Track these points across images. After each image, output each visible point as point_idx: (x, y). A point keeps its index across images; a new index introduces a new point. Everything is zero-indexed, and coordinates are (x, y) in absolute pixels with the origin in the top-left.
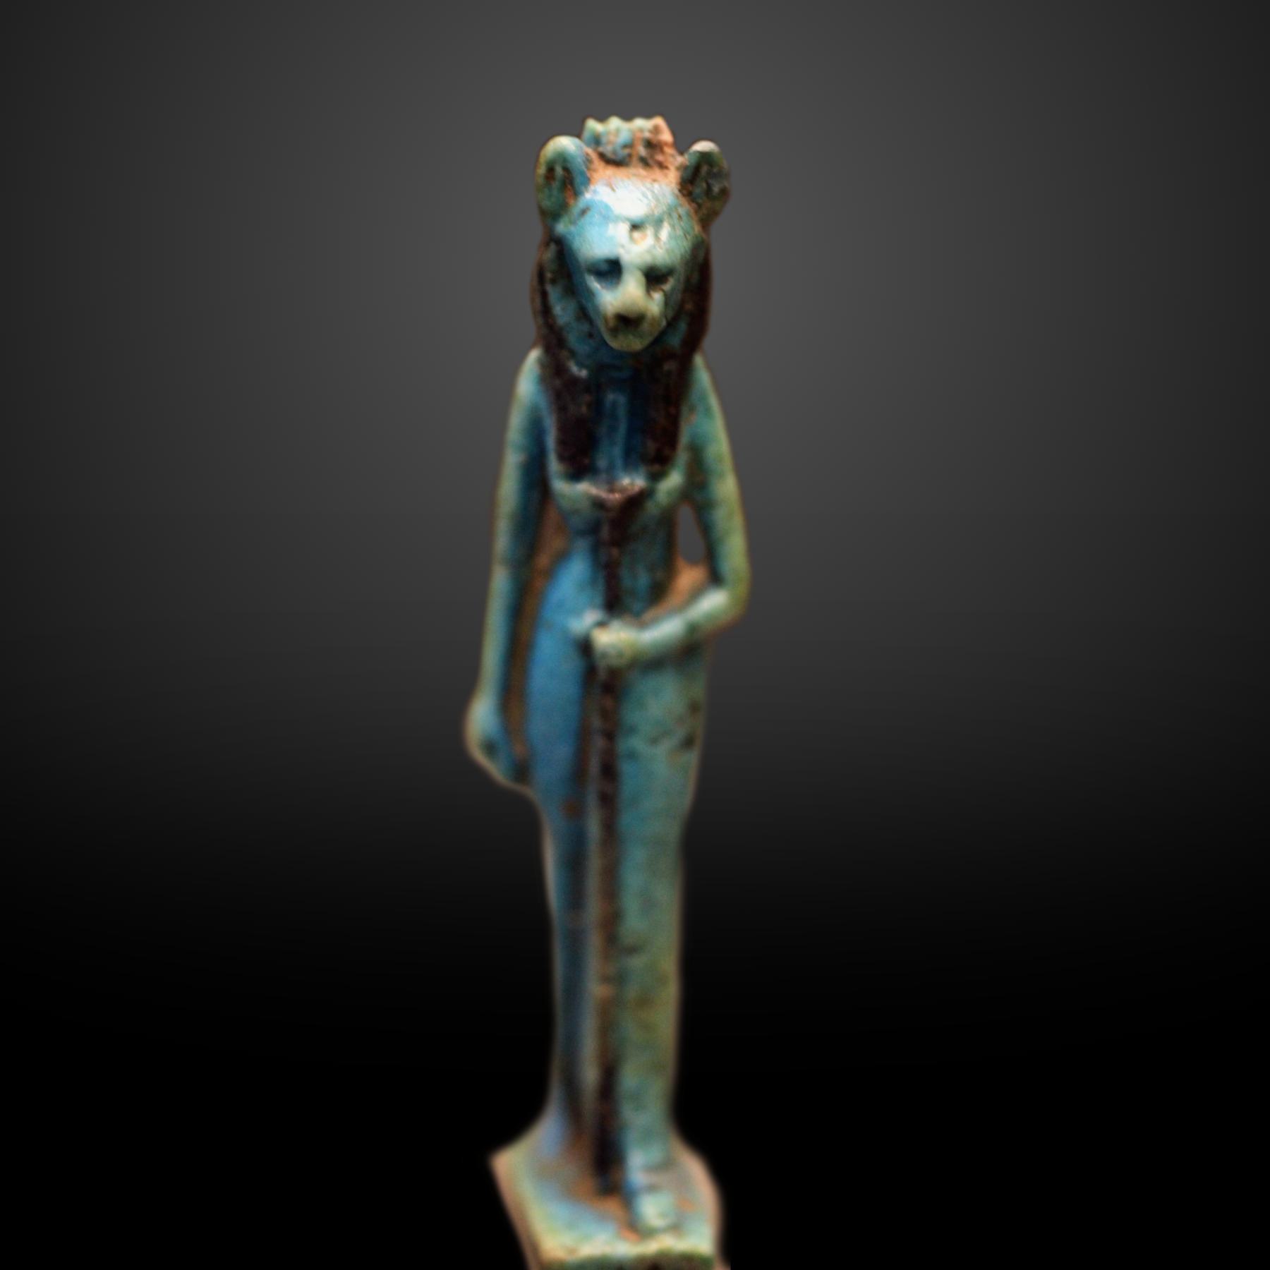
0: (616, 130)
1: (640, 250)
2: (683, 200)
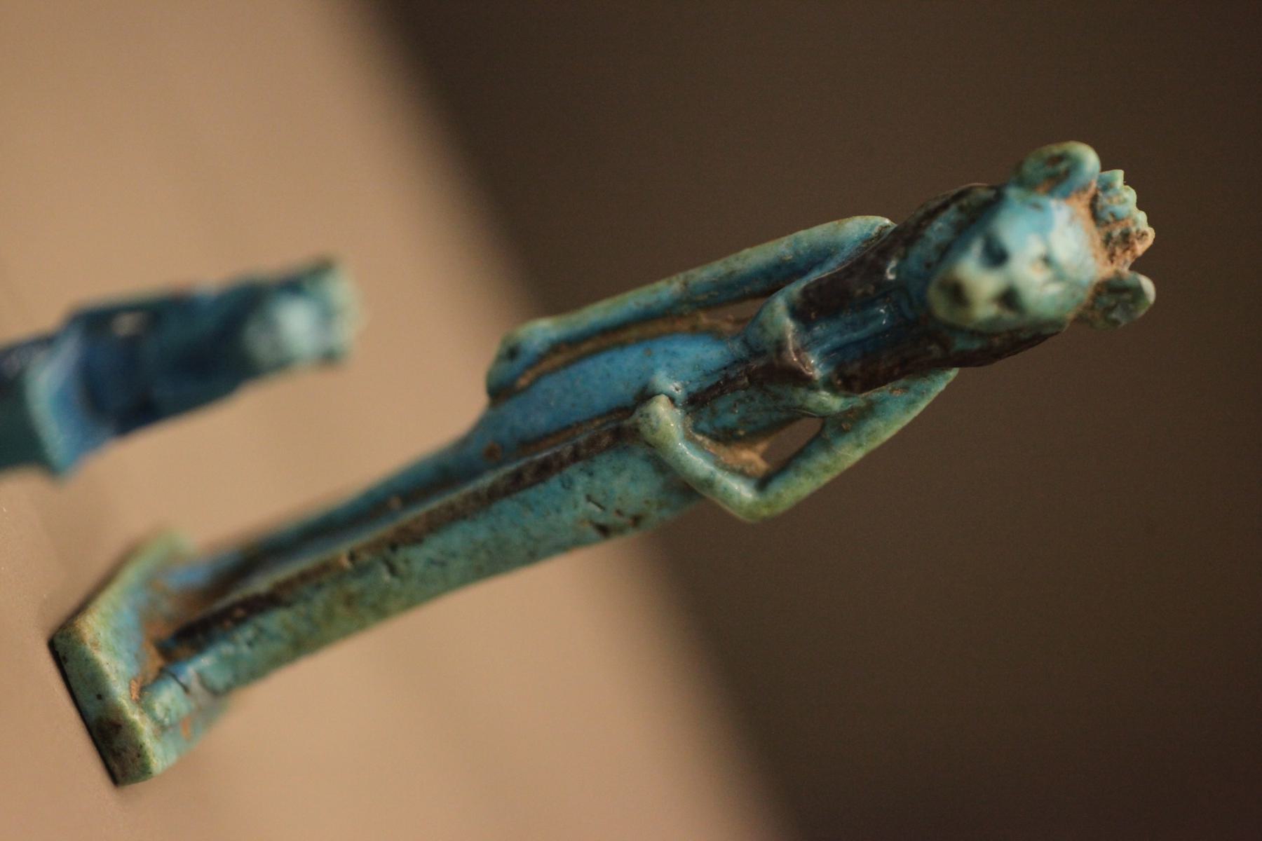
0: (1125, 199)
2: (1090, 292)
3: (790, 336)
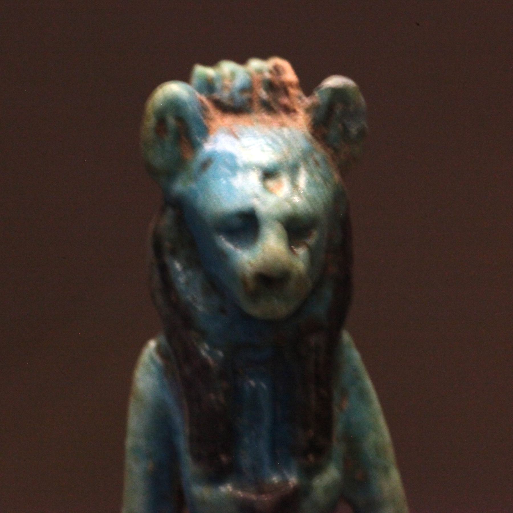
0: (230, 74)
2: (318, 146)
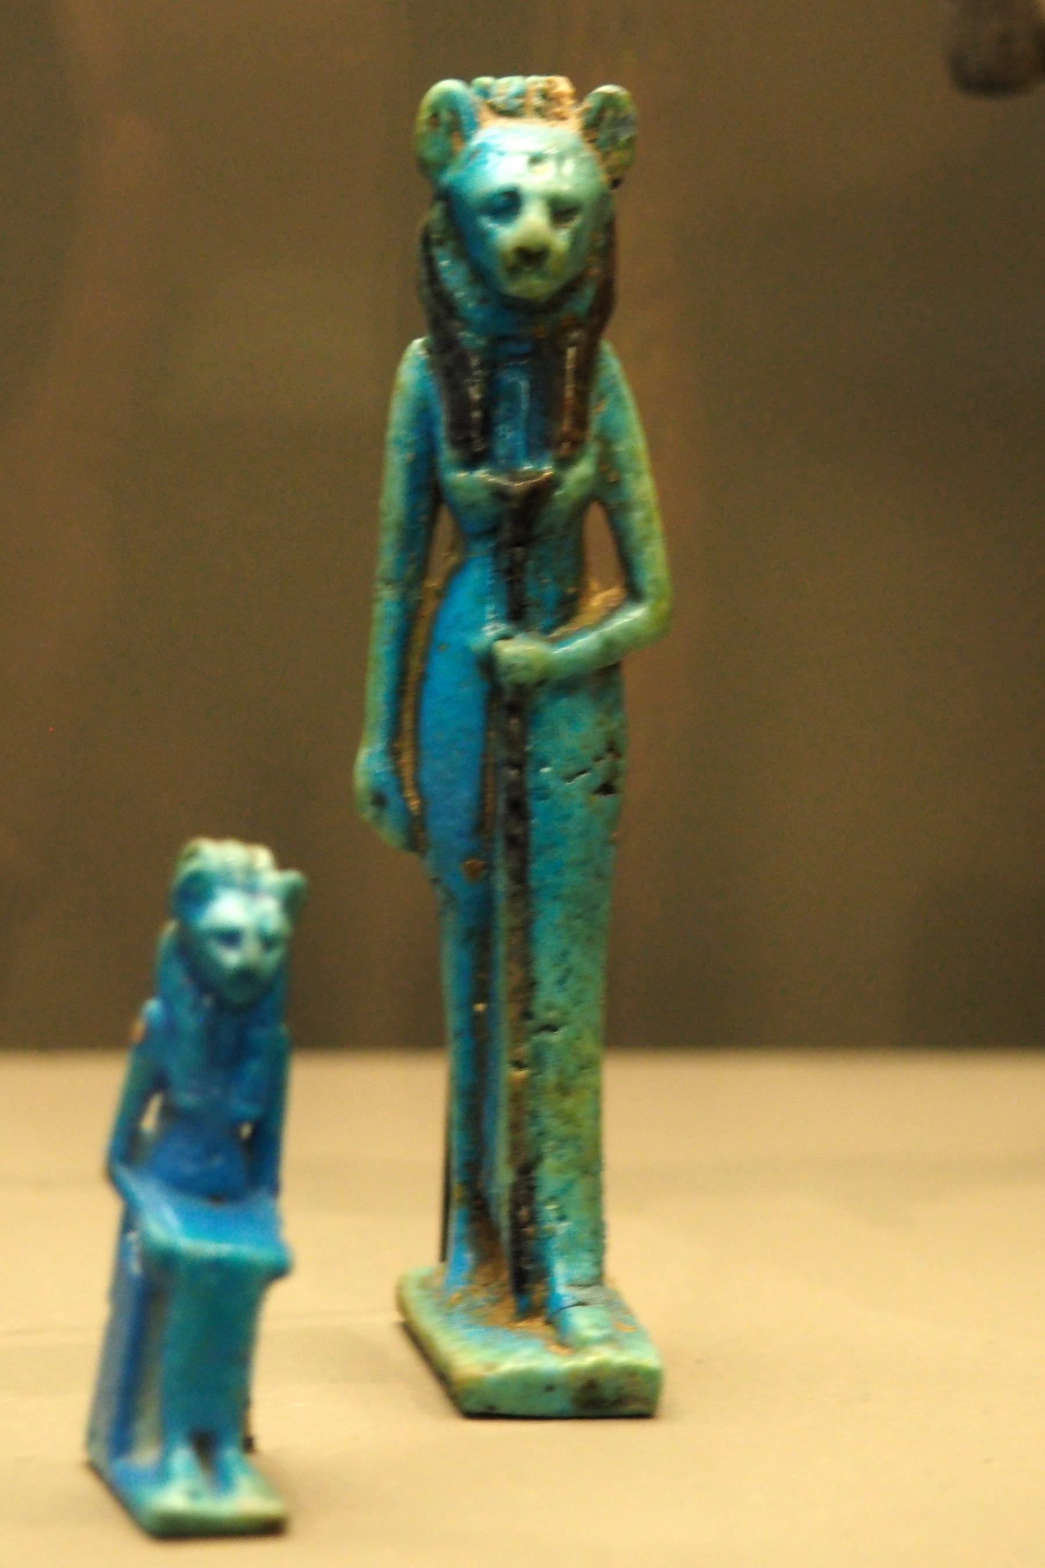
1: (541, 181)
3: (492, 479)
